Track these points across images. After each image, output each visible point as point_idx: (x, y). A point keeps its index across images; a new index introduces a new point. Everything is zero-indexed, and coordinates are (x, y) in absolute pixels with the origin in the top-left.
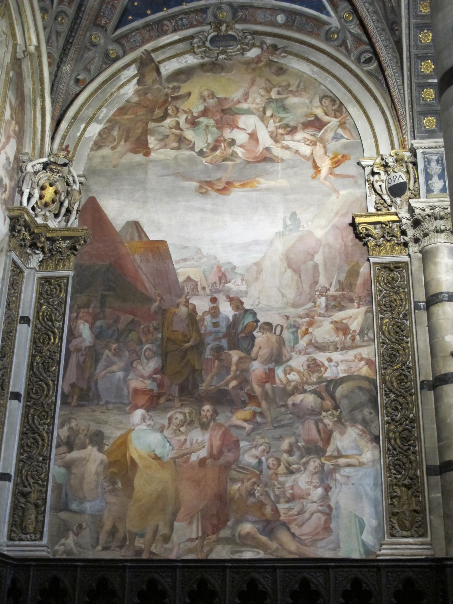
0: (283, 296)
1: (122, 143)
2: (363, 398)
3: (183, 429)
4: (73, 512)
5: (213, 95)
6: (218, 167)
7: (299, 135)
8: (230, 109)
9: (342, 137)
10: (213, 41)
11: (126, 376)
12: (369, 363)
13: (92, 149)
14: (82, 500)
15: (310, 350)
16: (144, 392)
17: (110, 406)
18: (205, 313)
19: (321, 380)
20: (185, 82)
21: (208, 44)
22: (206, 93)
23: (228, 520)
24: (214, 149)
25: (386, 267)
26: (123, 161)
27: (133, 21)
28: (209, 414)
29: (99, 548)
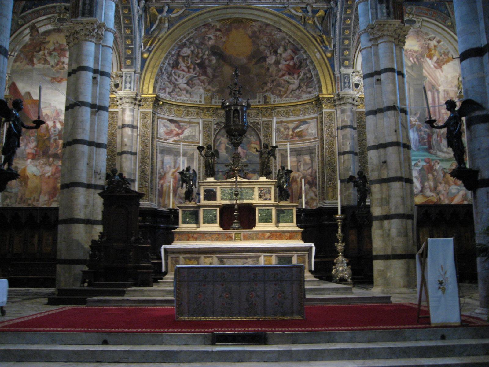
1: (24, 60)
3: (43, 166)
4: (9, 192)
6: (58, 72)
8: (63, 49)
10: (58, 20)
11: (25, 148)
13: (13, 62)
14: (11, 189)
16: (31, 154)
17: (20, 158)
18: (51, 127)
20: (48, 36)
21: (56, 21)
22: (55, 42)
23: (56, 195)
24: (57, 65)
26: (25, 68)
27: (28, 10)
28: (52, 161)
29: (17, 203)
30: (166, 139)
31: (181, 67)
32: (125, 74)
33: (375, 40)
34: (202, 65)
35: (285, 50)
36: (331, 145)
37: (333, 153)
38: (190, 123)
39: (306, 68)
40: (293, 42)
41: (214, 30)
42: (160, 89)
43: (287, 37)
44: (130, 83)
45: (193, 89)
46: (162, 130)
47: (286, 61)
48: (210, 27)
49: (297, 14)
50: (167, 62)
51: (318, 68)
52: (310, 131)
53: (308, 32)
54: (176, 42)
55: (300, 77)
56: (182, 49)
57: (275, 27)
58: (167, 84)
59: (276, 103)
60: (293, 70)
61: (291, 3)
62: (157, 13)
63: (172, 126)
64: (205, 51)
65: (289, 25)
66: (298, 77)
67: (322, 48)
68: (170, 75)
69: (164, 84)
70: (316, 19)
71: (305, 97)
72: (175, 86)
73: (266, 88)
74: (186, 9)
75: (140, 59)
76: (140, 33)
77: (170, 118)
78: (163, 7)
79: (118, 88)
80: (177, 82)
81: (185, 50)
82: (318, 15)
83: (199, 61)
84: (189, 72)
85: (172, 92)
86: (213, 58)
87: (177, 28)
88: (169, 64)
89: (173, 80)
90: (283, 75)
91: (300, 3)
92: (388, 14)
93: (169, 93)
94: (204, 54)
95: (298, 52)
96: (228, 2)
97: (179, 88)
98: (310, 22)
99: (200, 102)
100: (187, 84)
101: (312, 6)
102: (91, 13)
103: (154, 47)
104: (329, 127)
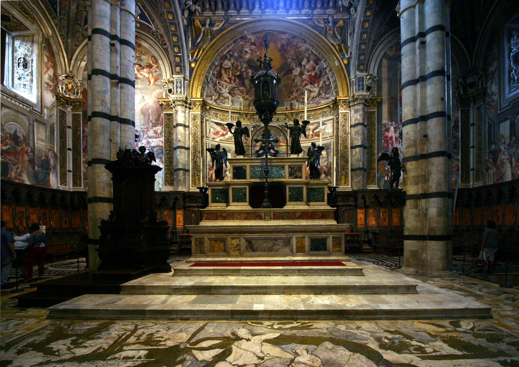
0: (141, 122)
2: (160, 151)
7: (145, 70)
9: (157, 72)
12: (162, 142)
15: (147, 138)
19: (150, 146)
25: (167, 114)
31: (223, 78)
32: (176, 80)
35: (308, 61)
36: (345, 141)
37: (346, 147)
39: (325, 77)
40: (315, 53)
41: (249, 44)
43: (311, 48)
48: (246, 40)
49: (320, 25)
53: (329, 41)
54: (218, 53)
56: (224, 61)
57: (301, 38)
58: (213, 93)
60: (314, 80)
61: (315, 14)
62: (201, 27)
64: (243, 64)
67: (340, 56)
68: (215, 85)
69: (210, 92)
70: (335, 29)
72: (220, 95)
74: (225, 22)
75: (188, 68)
78: (206, 19)
79: (172, 93)
80: (221, 91)
81: (226, 62)
82: (337, 25)
85: (217, 99)
87: (218, 40)
88: (213, 74)
89: (218, 89)
91: (323, 14)
93: (215, 101)
95: (319, 62)
96: (261, 15)
97: (223, 97)
98: (331, 32)
103: (199, 57)
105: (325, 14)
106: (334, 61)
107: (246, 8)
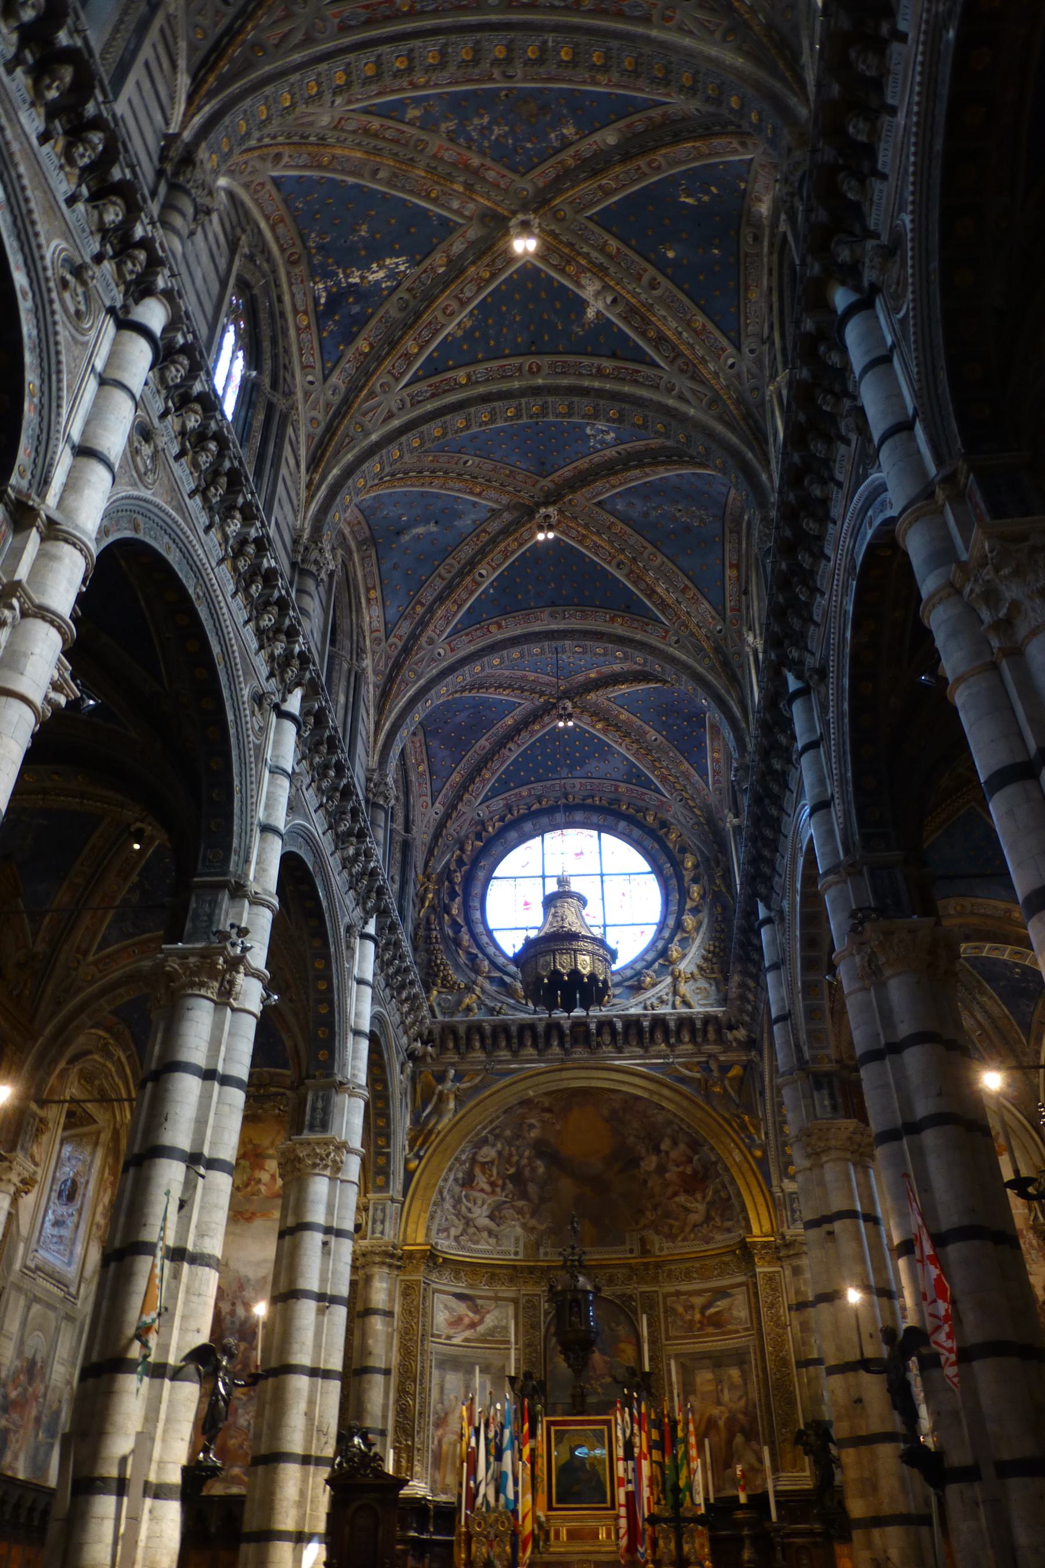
5: (251, 1141)
24: (247, 1185)
30: (449, 1338)
33: (815, 1155)
34: (518, 1179)
35: (675, 1143)
36: (779, 1344)
37: (784, 1362)
38: (497, 1299)
42: (439, 1231)
43: (677, 1121)
44: (383, 1222)
45: (502, 1227)
46: (441, 1318)
47: (678, 1166)
50: (452, 1177)
51: (740, 1182)
52: (735, 1313)
53: (715, 1110)
55: (708, 1199)
56: (480, 1148)
59: (665, 1252)
60: (694, 1183)
62: (434, 1083)
63: (462, 1308)
65: (677, 1098)
66: (704, 1198)
68: (458, 1201)
70: (726, 1082)
71: (721, 1240)
72: (468, 1222)
73: (643, 1221)
76: (402, 1122)
77: (458, 1291)
82: (730, 1074)
83: (512, 1171)
84: (493, 1192)
86: (539, 1163)
88: (456, 1180)
89: (464, 1209)
90: (675, 1194)
92: (834, 1108)
93: (457, 1239)
94: (521, 1157)
98: (717, 1089)
99: (516, 1253)
100: (491, 1217)
101: (717, 1060)
102: (324, 1126)
104: (772, 1306)
105: (700, 1053)
106: (731, 1154)
107: (532, 1046)
